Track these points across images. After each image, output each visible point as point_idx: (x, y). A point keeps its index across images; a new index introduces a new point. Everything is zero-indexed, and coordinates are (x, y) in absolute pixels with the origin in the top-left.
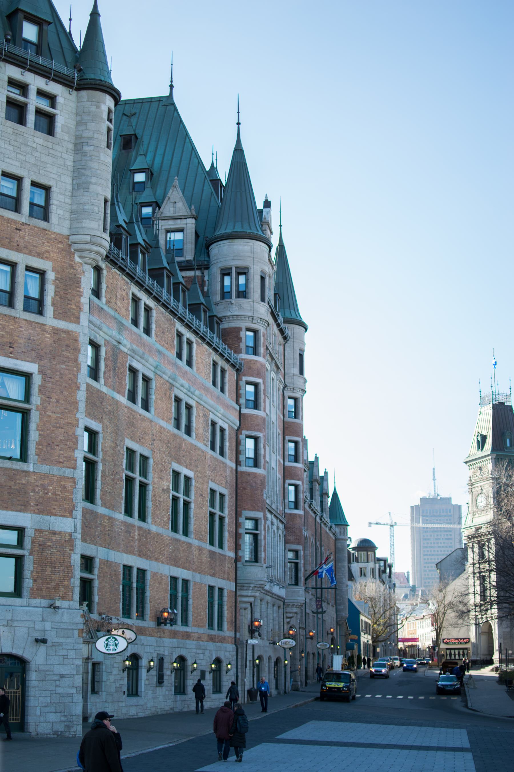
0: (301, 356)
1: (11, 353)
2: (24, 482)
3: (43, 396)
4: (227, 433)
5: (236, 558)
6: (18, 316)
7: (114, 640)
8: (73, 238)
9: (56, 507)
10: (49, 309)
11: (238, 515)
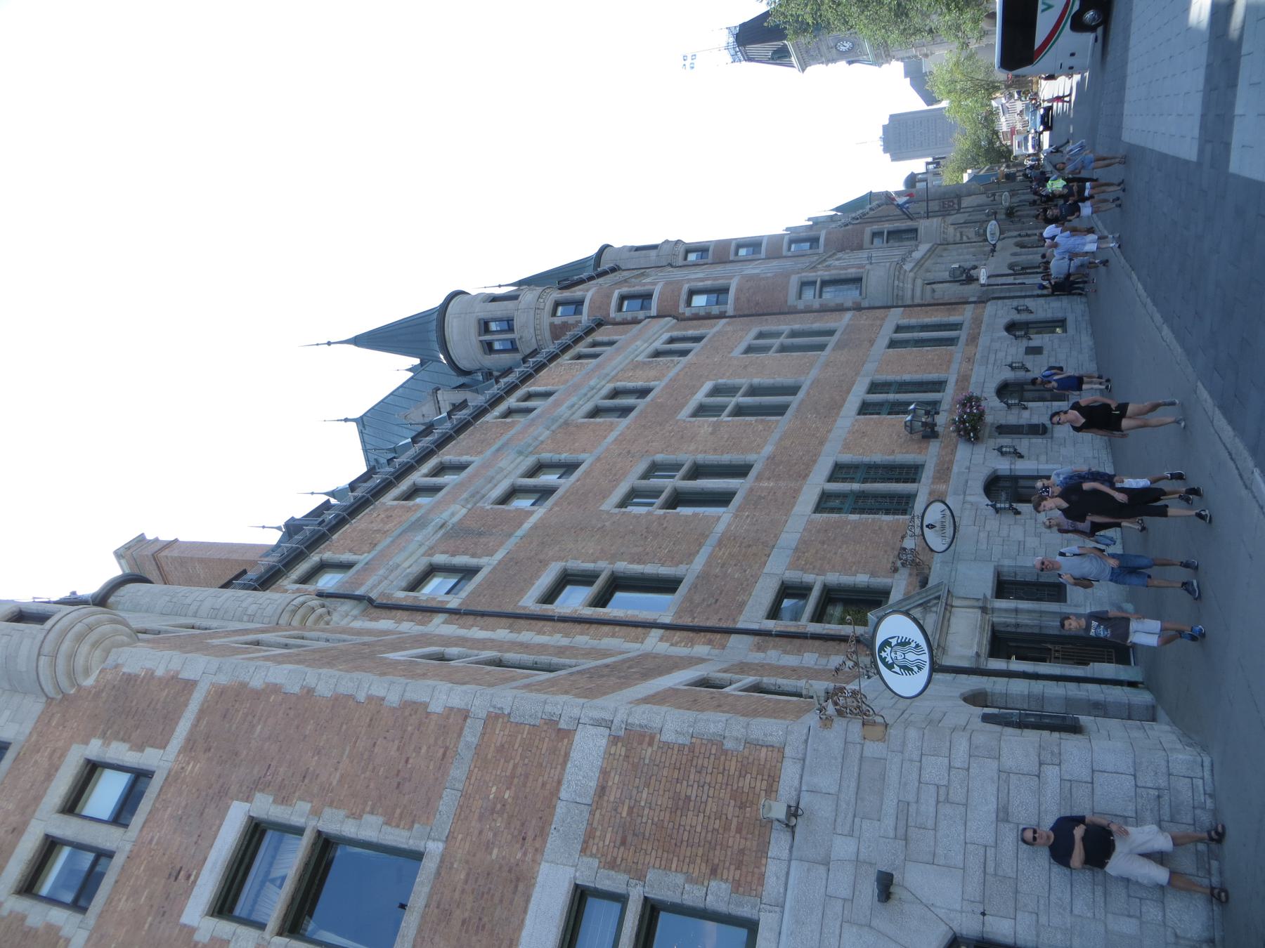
0: (638, 249)
1: (189, 876)
2: (463, 876)
3: (297, 794)
4: (676, 334)
5: (854, 309)
6: (128, 847)
7: (888, 649)
8: (49, 688)
9: (540, 780)
10: (148, 758)
11: (793, 311)
